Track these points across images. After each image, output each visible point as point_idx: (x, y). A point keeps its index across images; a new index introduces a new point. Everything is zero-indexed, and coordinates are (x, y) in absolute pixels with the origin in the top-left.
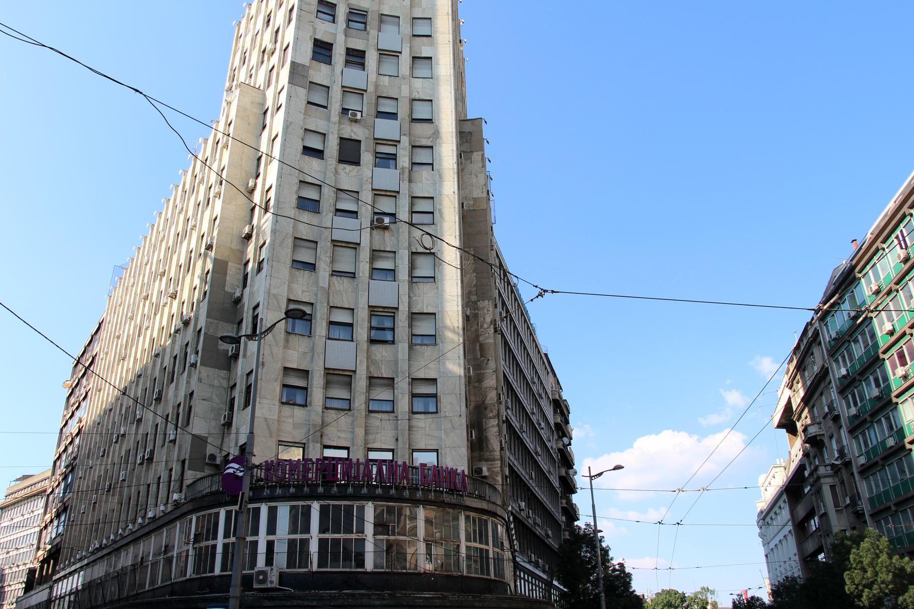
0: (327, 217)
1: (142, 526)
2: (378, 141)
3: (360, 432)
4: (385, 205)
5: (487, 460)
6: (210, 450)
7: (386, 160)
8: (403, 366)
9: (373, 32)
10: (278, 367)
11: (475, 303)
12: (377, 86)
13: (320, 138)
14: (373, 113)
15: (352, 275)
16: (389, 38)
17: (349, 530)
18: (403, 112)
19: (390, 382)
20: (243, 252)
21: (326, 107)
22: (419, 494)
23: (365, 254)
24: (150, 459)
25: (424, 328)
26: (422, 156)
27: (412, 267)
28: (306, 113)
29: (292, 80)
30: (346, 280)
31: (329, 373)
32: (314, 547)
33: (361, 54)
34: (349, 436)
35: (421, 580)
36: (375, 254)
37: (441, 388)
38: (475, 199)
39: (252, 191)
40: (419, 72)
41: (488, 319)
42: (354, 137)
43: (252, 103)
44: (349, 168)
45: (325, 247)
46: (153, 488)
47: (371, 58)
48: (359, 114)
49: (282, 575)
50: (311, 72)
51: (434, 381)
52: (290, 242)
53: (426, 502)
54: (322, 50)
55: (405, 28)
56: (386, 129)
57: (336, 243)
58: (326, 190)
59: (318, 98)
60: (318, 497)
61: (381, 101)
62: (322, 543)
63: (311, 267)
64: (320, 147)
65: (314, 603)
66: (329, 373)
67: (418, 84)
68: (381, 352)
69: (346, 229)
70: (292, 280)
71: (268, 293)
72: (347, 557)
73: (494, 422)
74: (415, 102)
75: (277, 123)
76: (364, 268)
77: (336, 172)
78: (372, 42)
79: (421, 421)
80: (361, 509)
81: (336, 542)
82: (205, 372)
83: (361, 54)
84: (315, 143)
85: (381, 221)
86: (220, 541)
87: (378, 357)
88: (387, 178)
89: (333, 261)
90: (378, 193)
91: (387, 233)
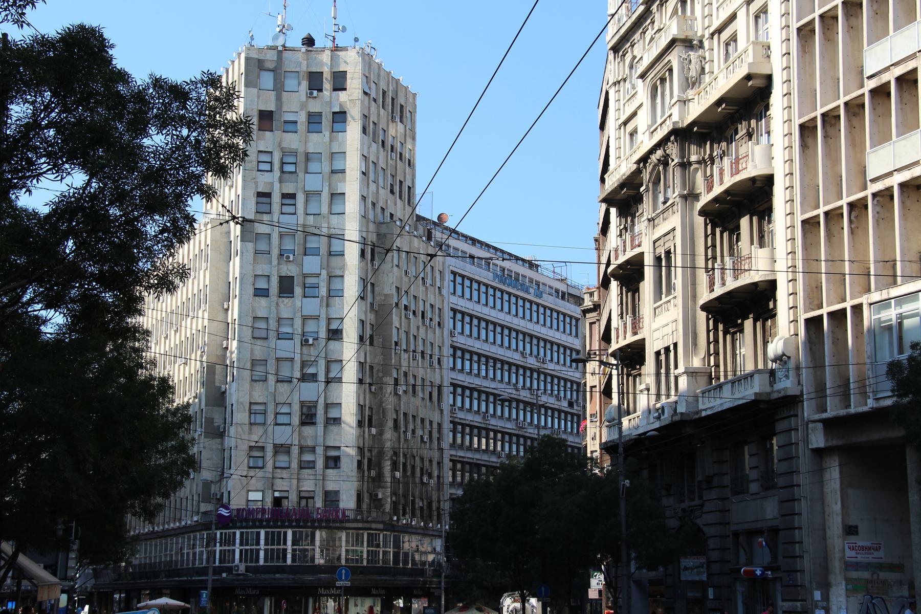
0: (273, 341)
1: (179, 528)
2: (305, 276)
3: (295, 482)
4: (311, 327)
5: (383, 488)
6: (213, 489)
7: (309, 291)
8: (320, 440)
9: (301, 175)
10: (246, 447)
11: (381, 378)
13: (265, 279)
14: (302, 252)
16: (312, 182)
17: (279, 544)
19: (313, 450)
20: (225, 356)
22: (316, 524)
23: (297, 365)
27: (328, 371)
28: (255, 261)
30: (286, 384)
31: (276, 446)
32: (262, 554)
33: (293, 196)
34: (288, 484)
36: (304, 364)
38: (385, 295)
39: (227, 310)
40: (336, 209)
41: (389, 391)
42: (290, 274)
43: (221, 234)
44: (286, 300)
47: (301, 198)
48: (291, 256)
49: (246, 567)
51: (339, 448)
53: (320, 528)
55: (326, 169)
56: (311, 264)
57: (278, 359)
58: (271, 322)
59: (263, 246)
60: (264, 527)
61: (309, 238)
62: (266, 551)
64: (266, 287)
65: (278, 575)
66: (276, 446)
67: (334, 219)
68: (308, 430)
70: (252, 389)
72: (278, 558)
73: (388, 463)
75: (235, 266)
77: (277, 304)
78: (300, 185)
80: (285, 534)
81: (272, 550)
83: (293, 196)
84: (262, 284)
86: (218, 548)
87: (306, 434)
88: (311, 306)
90: (305, 319)
91: (312, 348)
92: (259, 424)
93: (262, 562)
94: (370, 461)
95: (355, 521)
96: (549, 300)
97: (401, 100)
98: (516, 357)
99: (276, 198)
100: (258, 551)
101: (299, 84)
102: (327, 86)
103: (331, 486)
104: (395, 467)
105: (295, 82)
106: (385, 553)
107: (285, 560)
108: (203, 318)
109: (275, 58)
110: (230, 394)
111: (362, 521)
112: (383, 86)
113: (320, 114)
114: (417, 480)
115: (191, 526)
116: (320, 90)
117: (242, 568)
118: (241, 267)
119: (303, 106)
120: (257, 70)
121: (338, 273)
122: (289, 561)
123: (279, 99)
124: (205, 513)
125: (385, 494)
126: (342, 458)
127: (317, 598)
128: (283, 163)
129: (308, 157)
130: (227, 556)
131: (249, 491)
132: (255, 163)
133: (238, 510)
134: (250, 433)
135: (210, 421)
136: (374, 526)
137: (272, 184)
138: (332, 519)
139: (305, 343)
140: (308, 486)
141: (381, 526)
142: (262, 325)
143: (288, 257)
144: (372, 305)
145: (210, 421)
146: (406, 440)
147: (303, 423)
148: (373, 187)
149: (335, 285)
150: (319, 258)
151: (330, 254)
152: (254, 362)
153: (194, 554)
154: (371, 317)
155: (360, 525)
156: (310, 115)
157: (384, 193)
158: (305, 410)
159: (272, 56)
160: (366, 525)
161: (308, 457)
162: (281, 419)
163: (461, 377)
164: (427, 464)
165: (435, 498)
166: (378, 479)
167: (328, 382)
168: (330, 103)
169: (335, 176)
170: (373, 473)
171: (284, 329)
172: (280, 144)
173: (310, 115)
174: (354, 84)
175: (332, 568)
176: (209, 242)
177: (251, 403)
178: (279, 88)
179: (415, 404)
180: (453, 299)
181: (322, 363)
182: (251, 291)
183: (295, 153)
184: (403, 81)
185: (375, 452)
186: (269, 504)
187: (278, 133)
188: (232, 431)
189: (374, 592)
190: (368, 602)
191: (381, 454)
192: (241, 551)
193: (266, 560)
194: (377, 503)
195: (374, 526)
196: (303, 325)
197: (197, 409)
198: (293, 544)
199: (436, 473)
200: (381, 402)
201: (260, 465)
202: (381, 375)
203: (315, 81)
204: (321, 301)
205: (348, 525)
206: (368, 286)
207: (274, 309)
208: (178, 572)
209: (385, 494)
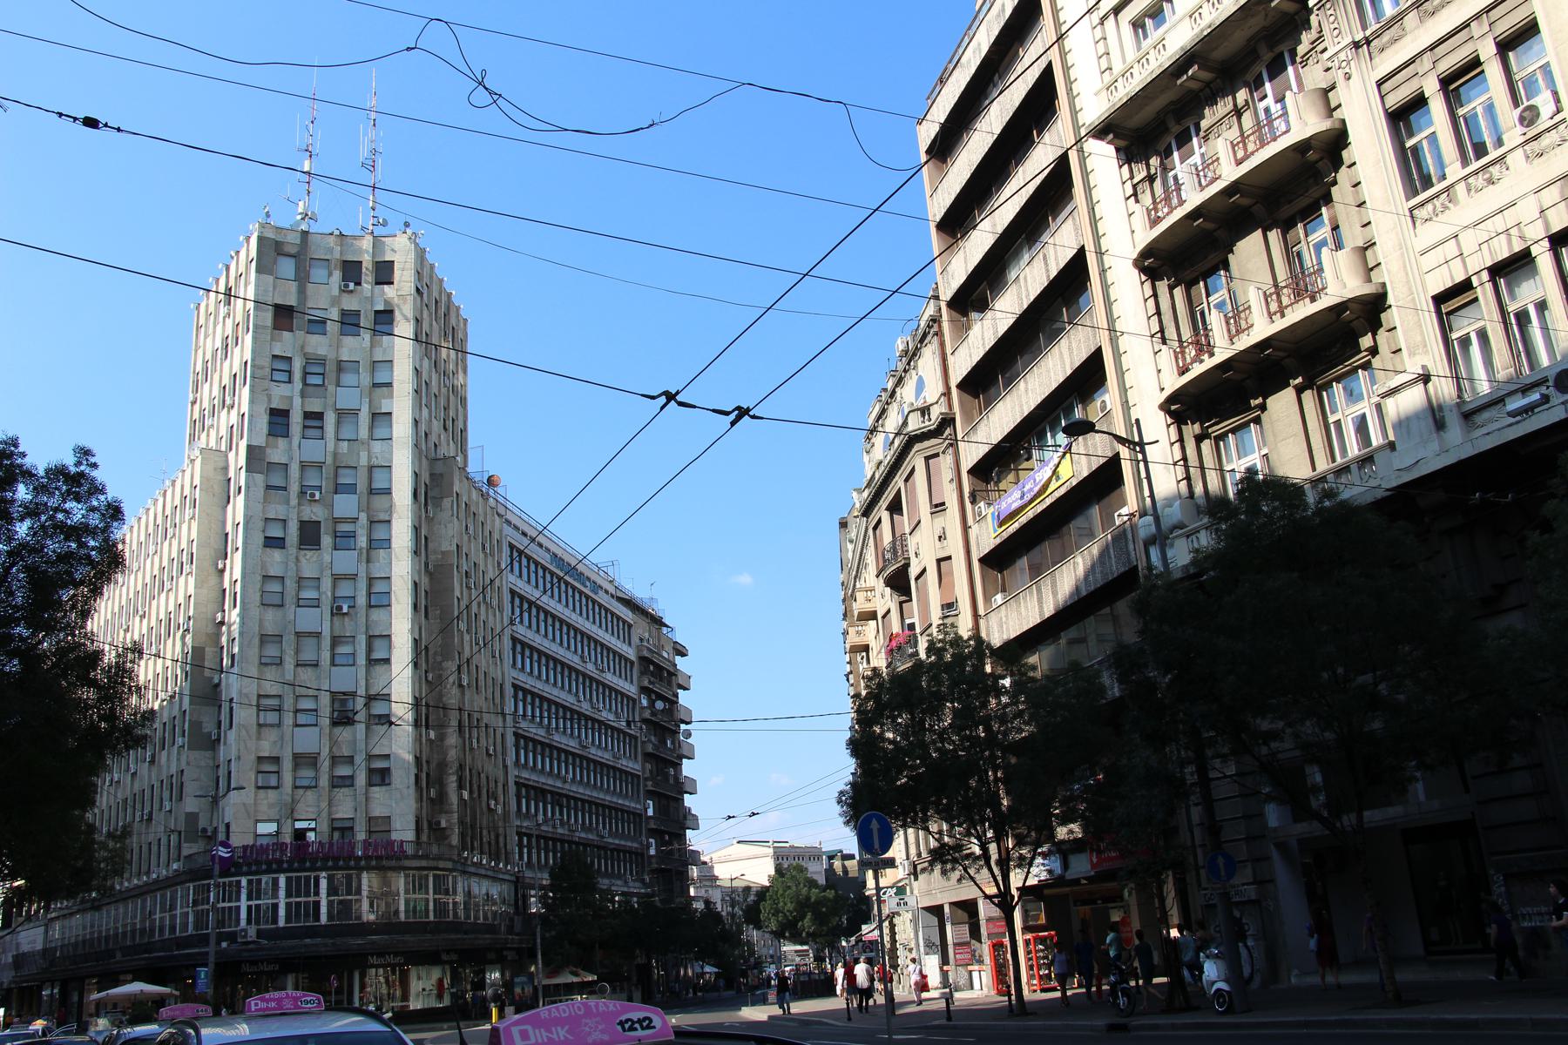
1: (146, 884)
2: (337, 521)
3: (324, 805)
4: (345, 589)
6: (202, 823)
7: (343, 540)
8: (361, 745)
9: (331, 388)
10: (253, 757)
12: (335, 454)
13: (280, 525)
14: (332, 487)
15: (316, 665)
16: (347, 398)
17: (307, 894)
18: (362, 486)
19: (350, 760)
20: (218, 635)
21: (285, 489)
23: (326, 643)
24: (150, 819)
25: (378, 708)
26: (379, 533)
27: (369, 650)
29: (250, 468)
30: (309, 669)
33: (319, 416)
35: (364, 929)
36: (336, 641)
37: (392, 764)
39: (222, 571)
40: (380, 432)
44: (309, 554)
45: (289, 641)
46: (154, 848)
47: (330, 419)
50: (268, 451)
51: (387, 757)
52: (256, 641)
53: (368, 869)
54: (278, 419)
55: (365, 380)
56: (345, 505)
58: (288, 582)
59: (277, 480)
60: (284, 871)
62: (288, 905)
63: (280, 662)
64: (280, 535)
67: (377, 447)
68: (344, 733)
69: (308, 619)
71: (240, 692)
72: (307, 915)
73: (454, 778)
75: (237, 509)
76: (326, 656)
77: (297, 559)
78: (330, 401)
79: (377, 792)
81: (298, 904)
82: (196, 754)
83: (319, 416)
84: (276, 532)
85: (339, 608)
88: (346, 561)
89: (297, 652)
90: (337, 579)
92: (272, 726)
93: (282, 923)
94: (430, 775)
95: (415, 857)
96: (602, 598)
97: (453, 321)
98: (574, 660)
99: (296, 418)
100: (275, 906)
101: (330, 274)
102: (368, 277)
103: (377, 811)
104: (461, 787)
105: (324, 272)
106: (455, 903)
107: (317, 918)
108: (187, 585)
110: (228, 685)
111: (425, 857)
112: (435, 294)
113: (357, 313)
114: (484, 805)
115: (167, 878)
116: (358, 283)
117: (252, 932)
118: (246, 507)
119: (335, 301)
120: (273, 254)
121: (383, 516)
122: (324, 919)
123: (302, 292)
124: (189, 857)
125: (449, 821)
126: (393, 770)
127: (364, 968)
128: (305, 374)
129: (340, 367)
131: (258, 821)
132: (268, 370)
133: (245, 848)
134: (259, 738)
135: (196, 725)
136: (441, 864)
137: (291, 398)
138: (385, 857)
139: (336, 612)
140: (344, 811)
141: (449, 865)
142: (275, 587)
143: (313, 495)
144: (427, 565)
145: (196, 725)
146: (472, 749)
147: (335, 723)
148: (425, 412)
149: (379, 533)
150: (355, 497)
151: (372, 492)
152: (264, 639)
153: (173, 917)
154: (425, 582)
155: (424, 863)
156: (344, 313)
157: (437, 426)
158: (337, 706)
159: (294, 239)
160: (432, 863)
161: (343, 771)
162: (302, 719)
163: (523, 677)
164: (492, 785)
165: (501, 831)
166: (439, 802)
167: (371, 662)
168: (371, 300)
169: (379, 391)
170: (433, 793)
171: (306, 594)
172: (302, 347)
173: (344, 313)
174: (404, 278)
175: (389, 926)
176: (197, 481)
177: (259, 696)
178: (302, 278)
179: (476, 702)
180: (512, 578)
181: (362, 640)
182: (261, 540)
183: (322, 361)
184: (456, 301)
185: (433, 765)
186: (287, 838)
187: (300, 334)
188: (232, 736)
189: (445, 957)
190: (436, 973)
191: (442, 765)
192: (249, 907)
193: (288, 919)
194: (438, 833)
195: (441, 864)
196: (334, 587)
197: (176, 712)
198: (329, 895)
200: (441, 696)
201: (273, 783)
202: (439, 659)
203: (351, 271)
204: (360, 554)
205: (407, 863)
206: (422, 543)
207: (292, 565)
208: (149, 947)
209: (449, 821)
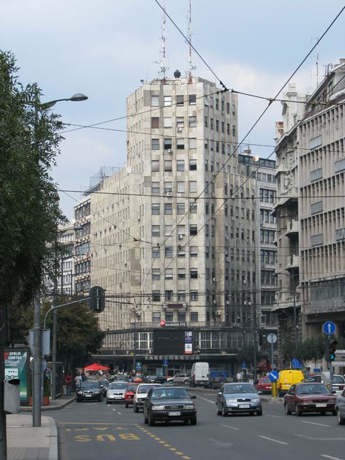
74: (191, 183)
85: (179, 237)
104: (227, 299)
109: (159, 89)
123: (162, 112)
130: (144, 345)
137: (159, 156)
194: (215, 316)
199: (252, 299)
209: (221, 312)
